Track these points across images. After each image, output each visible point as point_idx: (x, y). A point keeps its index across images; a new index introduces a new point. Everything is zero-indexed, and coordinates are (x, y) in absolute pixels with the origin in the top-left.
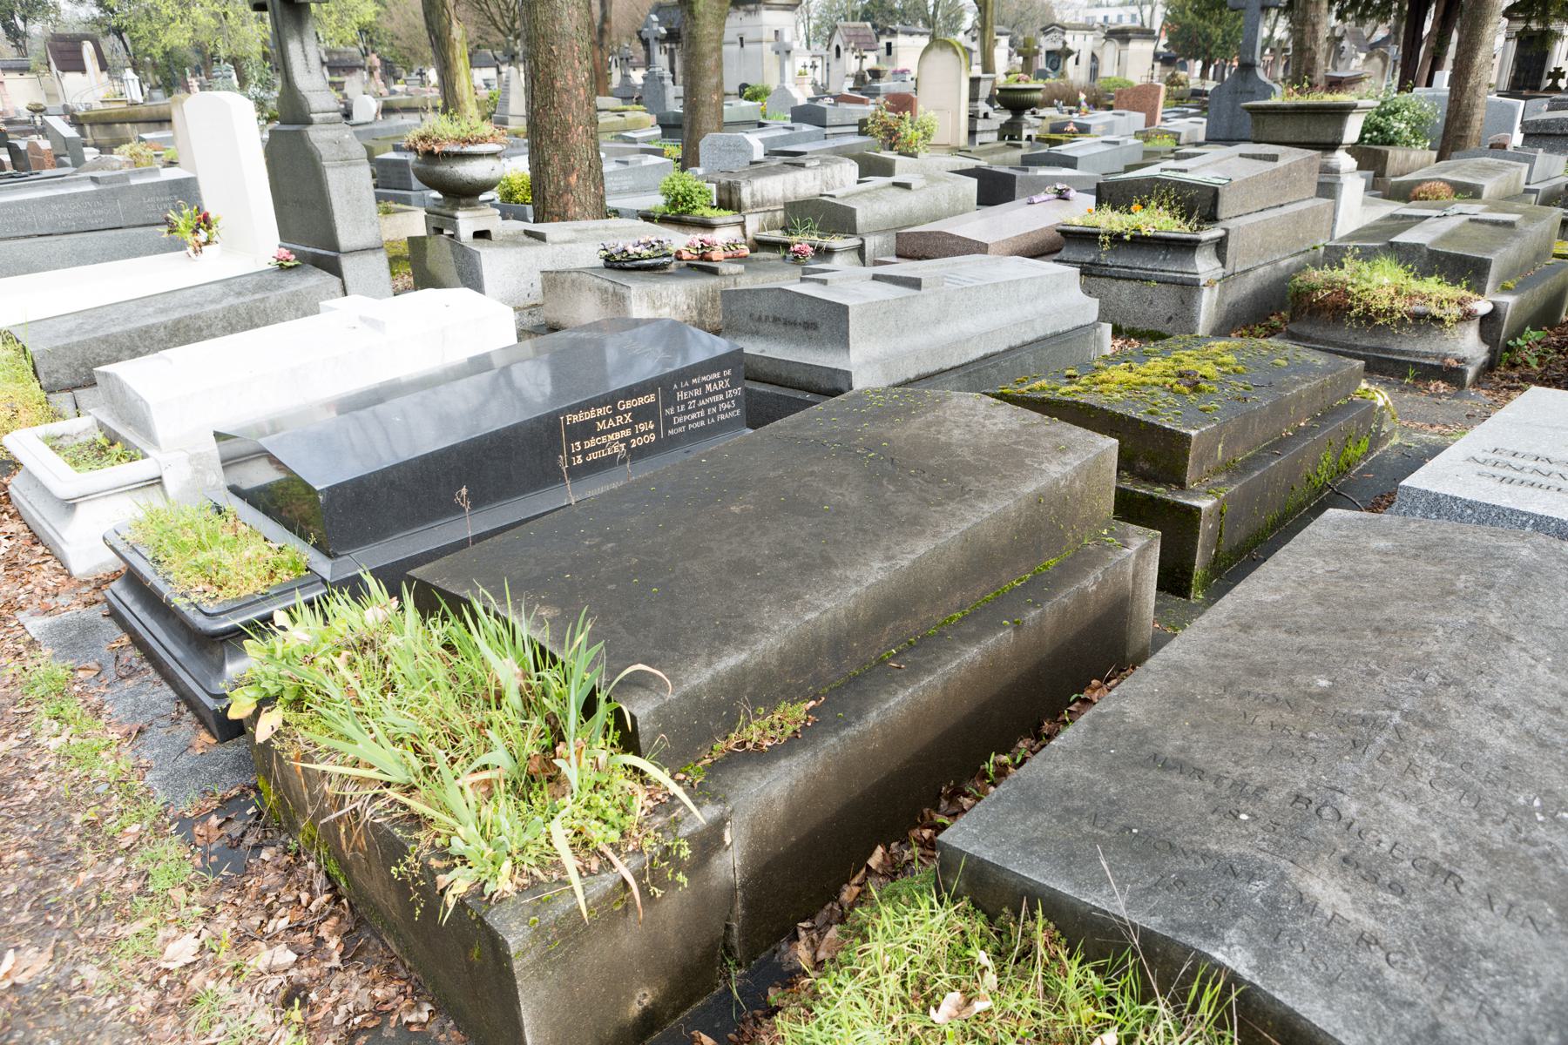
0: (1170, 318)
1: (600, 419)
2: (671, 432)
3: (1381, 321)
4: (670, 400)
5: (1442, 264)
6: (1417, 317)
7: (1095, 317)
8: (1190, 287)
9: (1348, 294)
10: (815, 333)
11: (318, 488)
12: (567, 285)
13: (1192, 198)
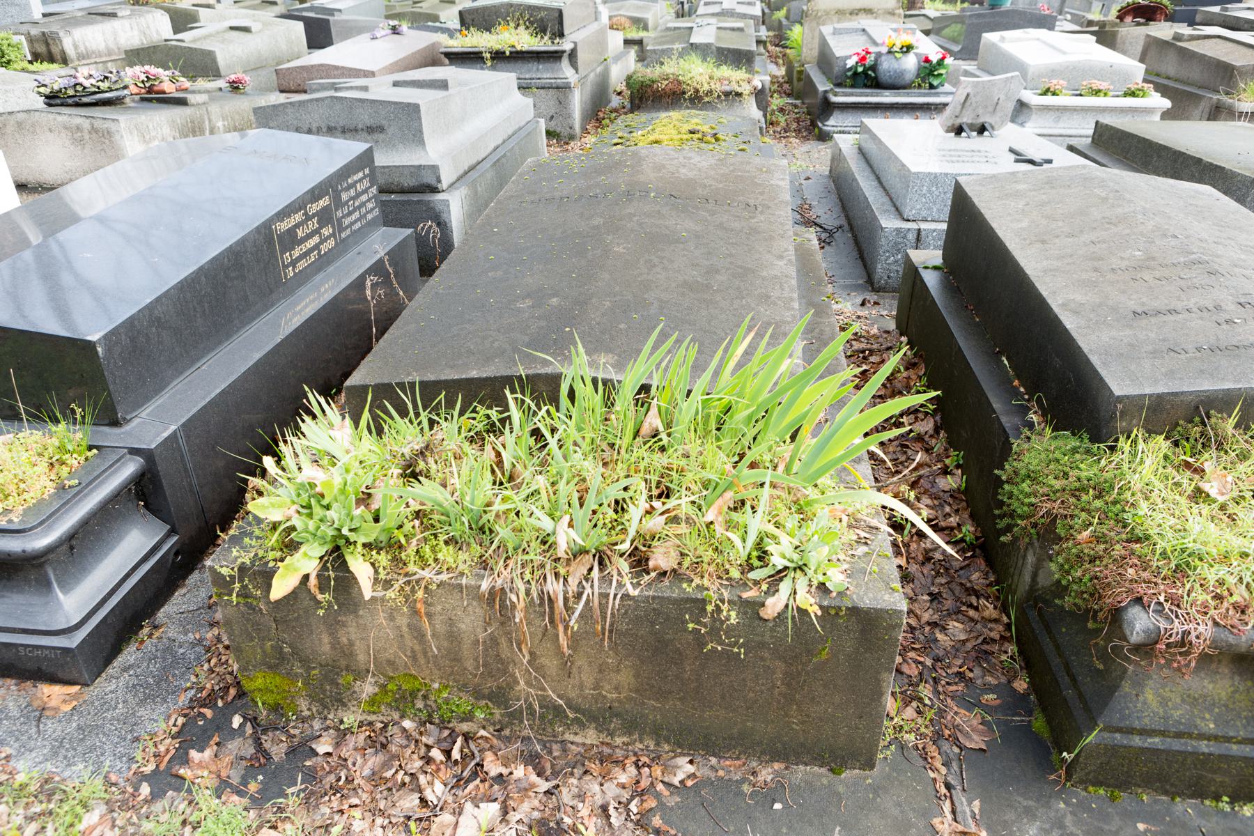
0: (552, 117)
1: (297, 226)
2: (343, 235)
3: (706, 99)
4: (339, 203)
5: (726, 56)
6: (727, 94)
7: (532, 115)
8: (563, 89)
9: (680, 83)
10: (381, 136)
11: (93, 337)
12: (9, 130)
13: (542, 19)
